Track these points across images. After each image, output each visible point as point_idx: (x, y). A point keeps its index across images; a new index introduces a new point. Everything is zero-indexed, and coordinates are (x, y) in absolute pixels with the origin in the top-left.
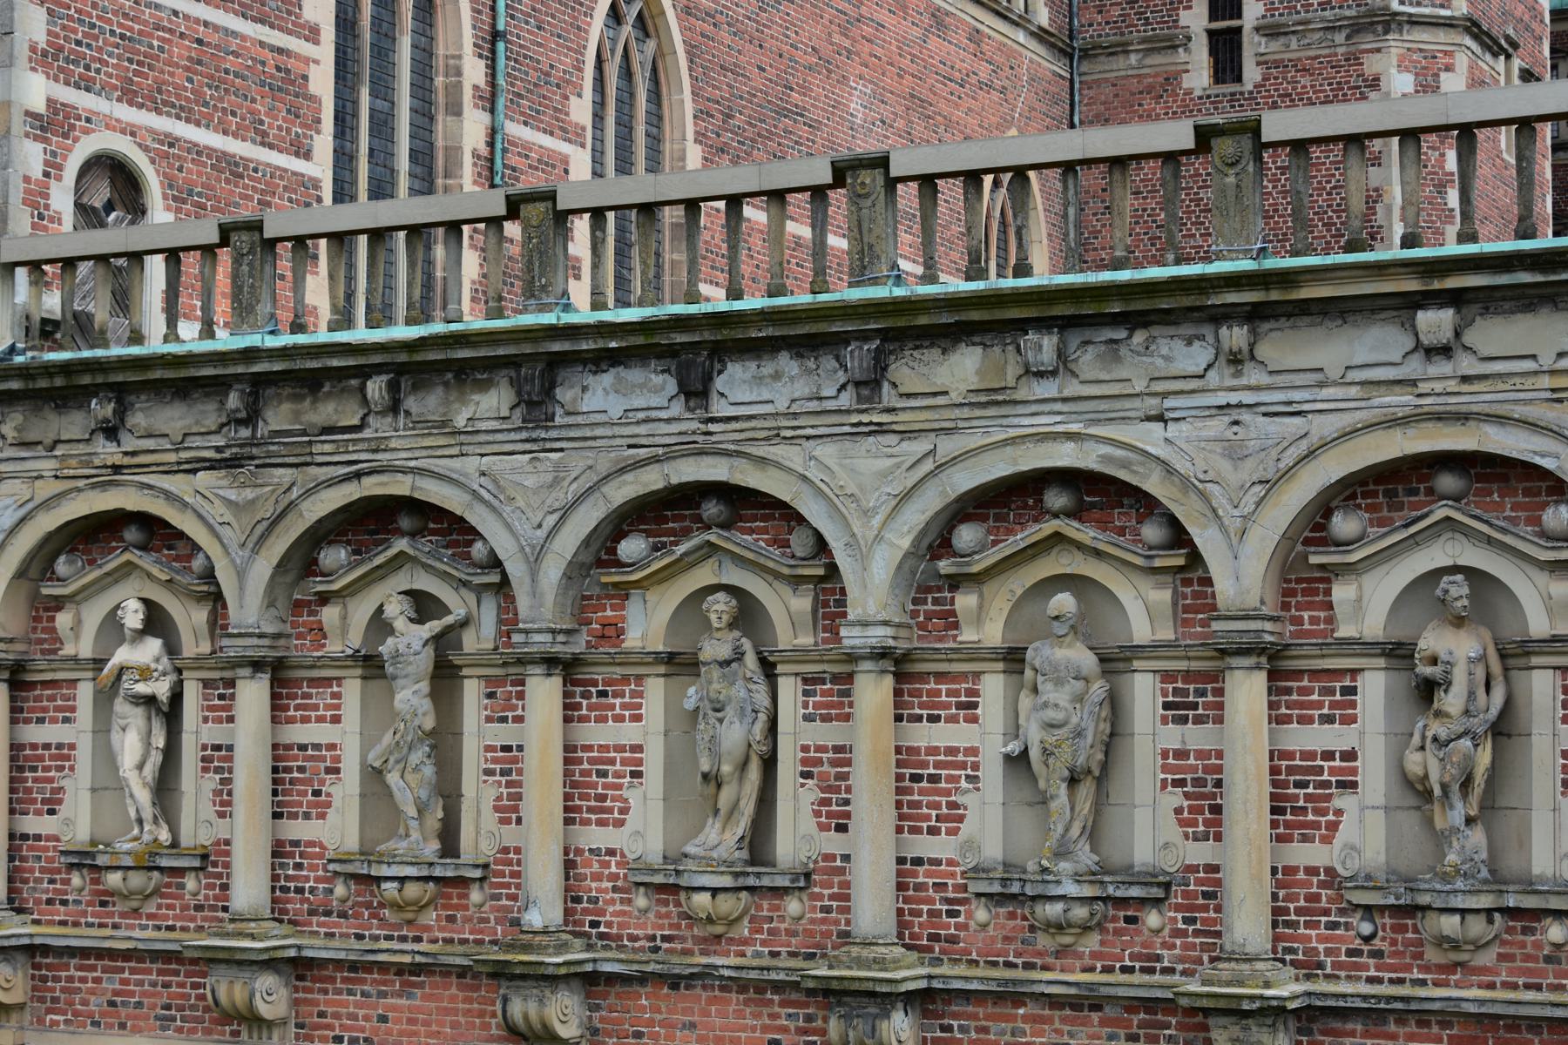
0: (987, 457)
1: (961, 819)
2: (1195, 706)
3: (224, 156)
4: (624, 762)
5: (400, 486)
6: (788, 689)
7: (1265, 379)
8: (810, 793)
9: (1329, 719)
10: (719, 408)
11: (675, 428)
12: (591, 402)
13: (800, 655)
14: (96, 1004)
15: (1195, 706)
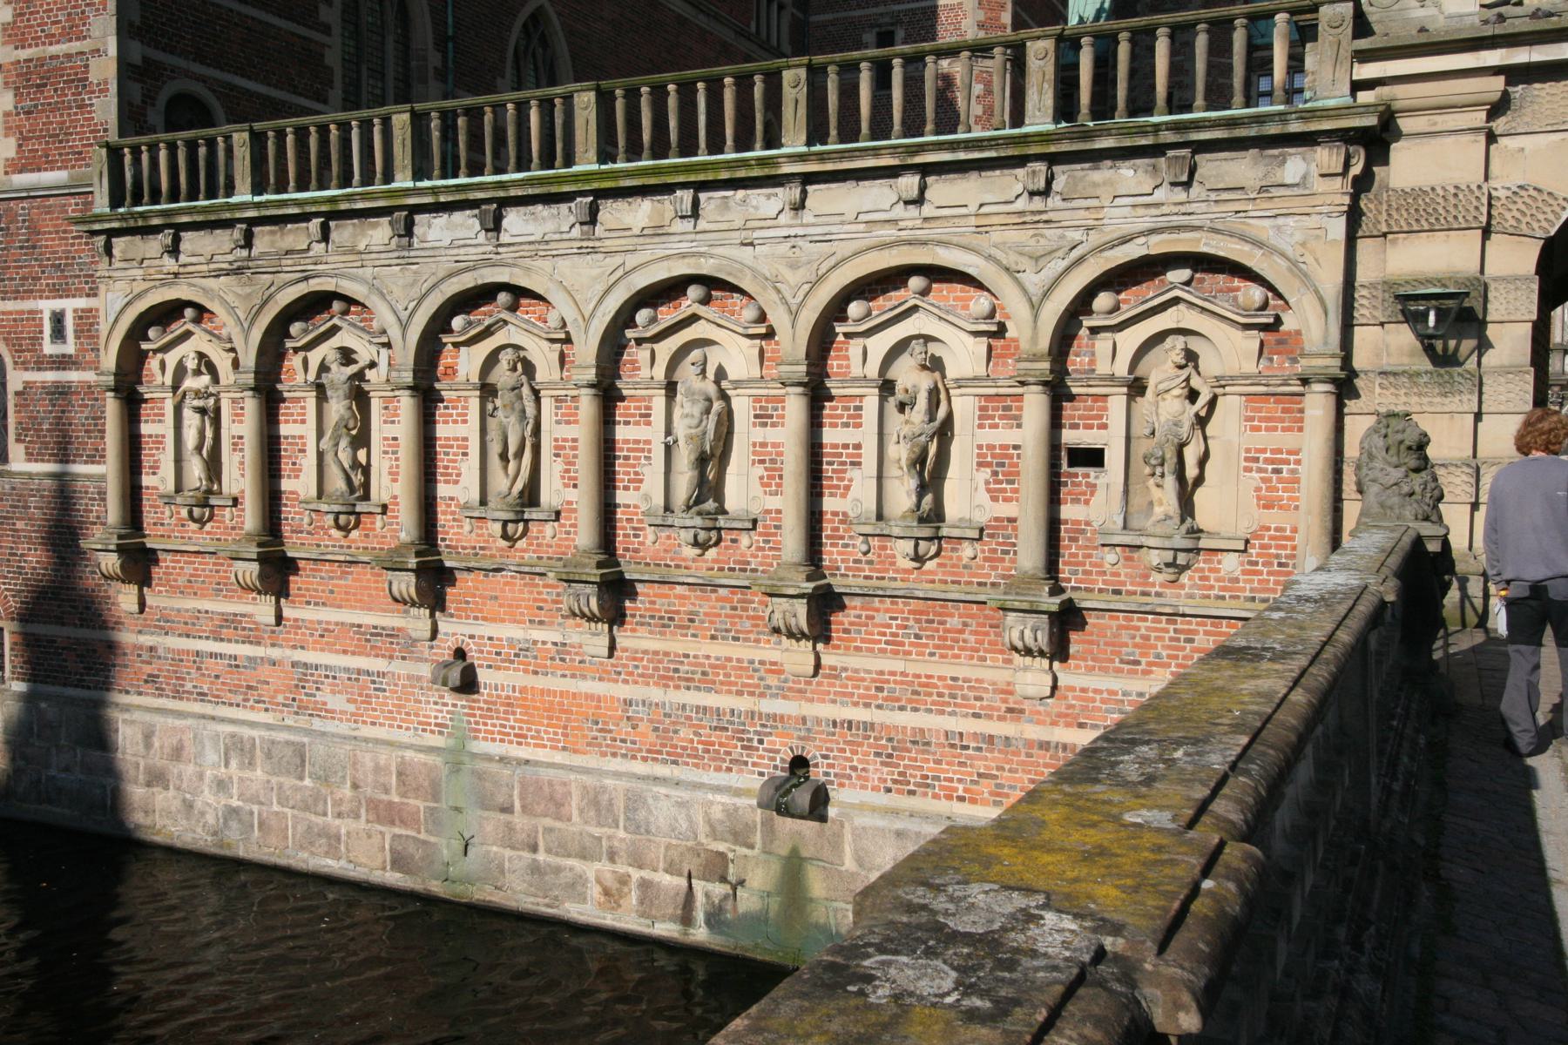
0: (652, 267)
1: (641, 481)
2: (771, 417)
3: (268, 98)
4: (458, 447)
5: (327, 285)
6: (546, 404)
7: (813, 220)
8: (559, 466)
9: (846, 425)
10: (504, 238)
11: (481, 250)
12: (433, 235)
13: (551, 385)
14: (181, 581)
15: (771, 417)
